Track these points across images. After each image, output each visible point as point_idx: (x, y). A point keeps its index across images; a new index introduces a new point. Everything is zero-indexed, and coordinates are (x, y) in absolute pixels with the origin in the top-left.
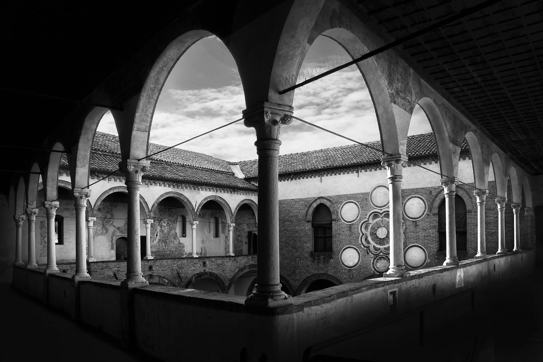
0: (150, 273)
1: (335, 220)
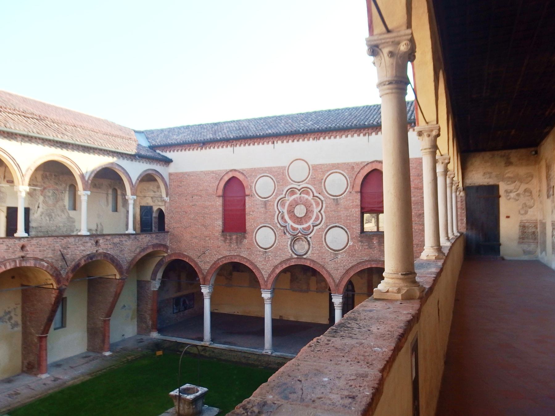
0: (22, 254)
1: (248, 195)
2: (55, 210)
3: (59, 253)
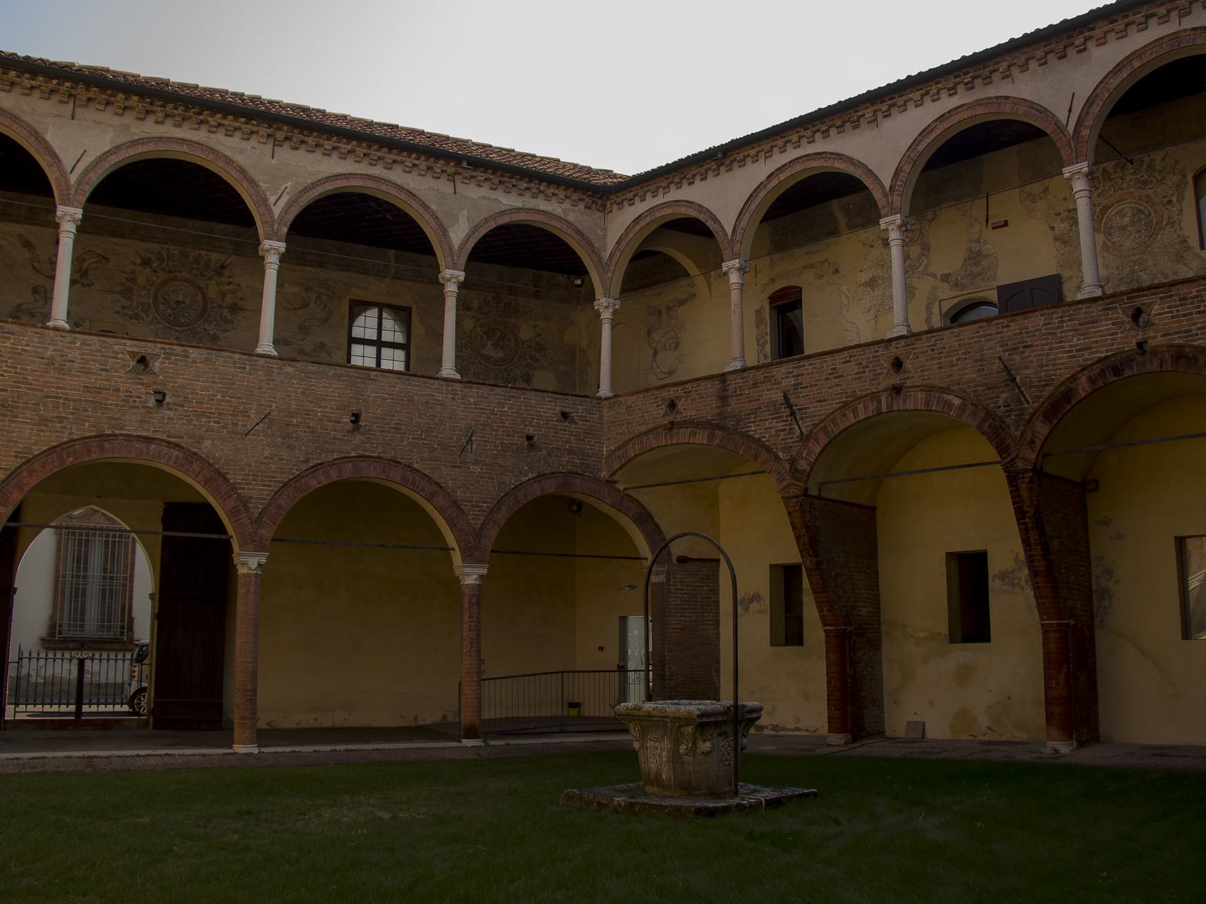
0: (896, 380)
3: (997, 365)
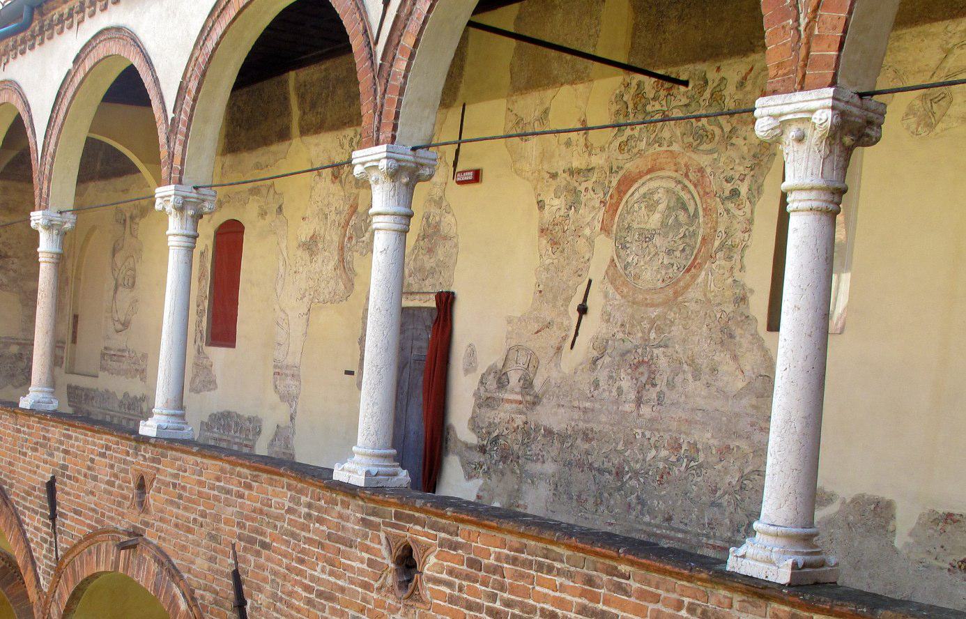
2: (677, 331)
